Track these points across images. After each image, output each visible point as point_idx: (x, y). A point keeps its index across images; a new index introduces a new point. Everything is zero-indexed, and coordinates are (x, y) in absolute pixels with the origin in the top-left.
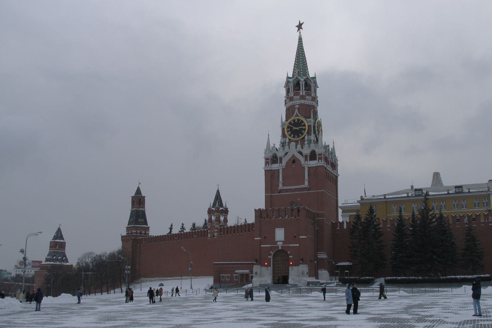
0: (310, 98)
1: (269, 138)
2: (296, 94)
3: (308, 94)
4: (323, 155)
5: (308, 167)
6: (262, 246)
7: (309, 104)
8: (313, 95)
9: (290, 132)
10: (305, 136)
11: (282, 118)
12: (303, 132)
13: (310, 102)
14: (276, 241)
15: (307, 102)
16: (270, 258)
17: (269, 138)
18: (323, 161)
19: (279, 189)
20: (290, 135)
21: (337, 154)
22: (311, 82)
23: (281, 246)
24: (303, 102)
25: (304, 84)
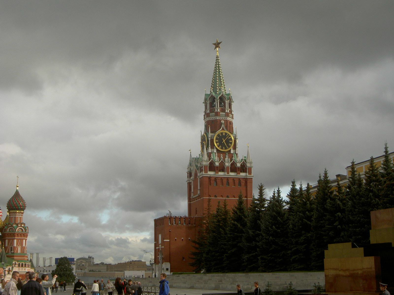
0: (214, 114)
1: (191, 155)
2: (212, 111)
4: (203, 167)
5: (200, 178)
6: (157, 248)
7: (213, 119)
8: (216, 111)
11: (201, 134)
13: (213, 118)
14: (159, 244)
15: (212, 118)
16: (158, 257)
17: (191, 155)
18: (204, 172)
19: (191, 198)
23: (161, 248)
24: (208, 119)
25: (208, 102)
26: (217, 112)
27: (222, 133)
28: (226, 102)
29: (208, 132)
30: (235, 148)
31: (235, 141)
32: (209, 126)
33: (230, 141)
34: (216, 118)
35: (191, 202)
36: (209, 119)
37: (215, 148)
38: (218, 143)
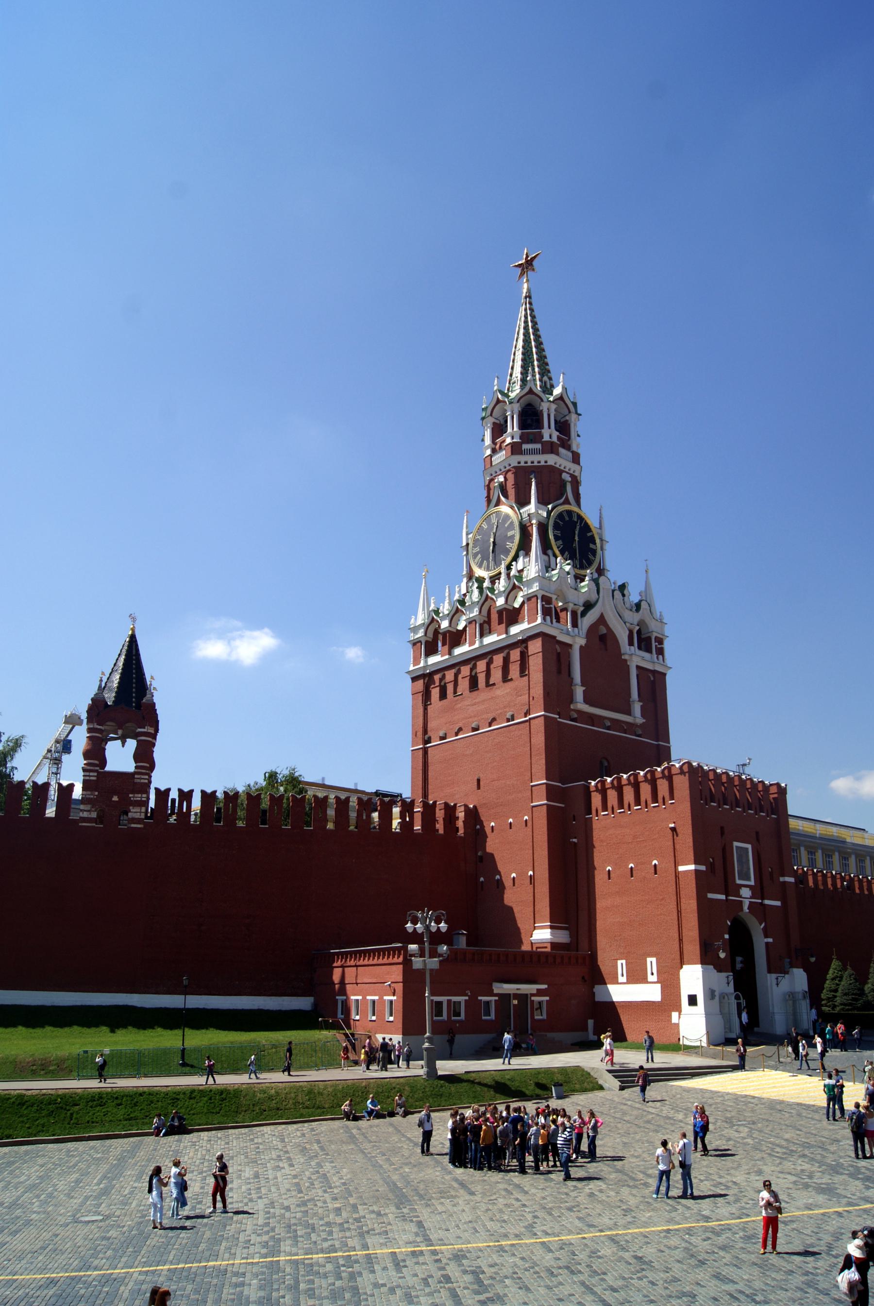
0: (539, 446)
3: (531, 437)
7: (536, 464)
8: (546, 438)
9: (479, 556)
10: (515, 558)
12: (509, 545)
20: (480, 566)
21: (659, 606)
22: (542, 400)
24: (515, 460)
26: (552, 443)
27: (570, 513)
28: (573, 420)
29: (522, 501)
30: (600, 571)
31: (602, 549)
32: (532, 476)
33: (591, 546)
34: (546, 462)
35: (428, 741)
36: (519, 463)
37: (550, 552)
38: (560, 542)
